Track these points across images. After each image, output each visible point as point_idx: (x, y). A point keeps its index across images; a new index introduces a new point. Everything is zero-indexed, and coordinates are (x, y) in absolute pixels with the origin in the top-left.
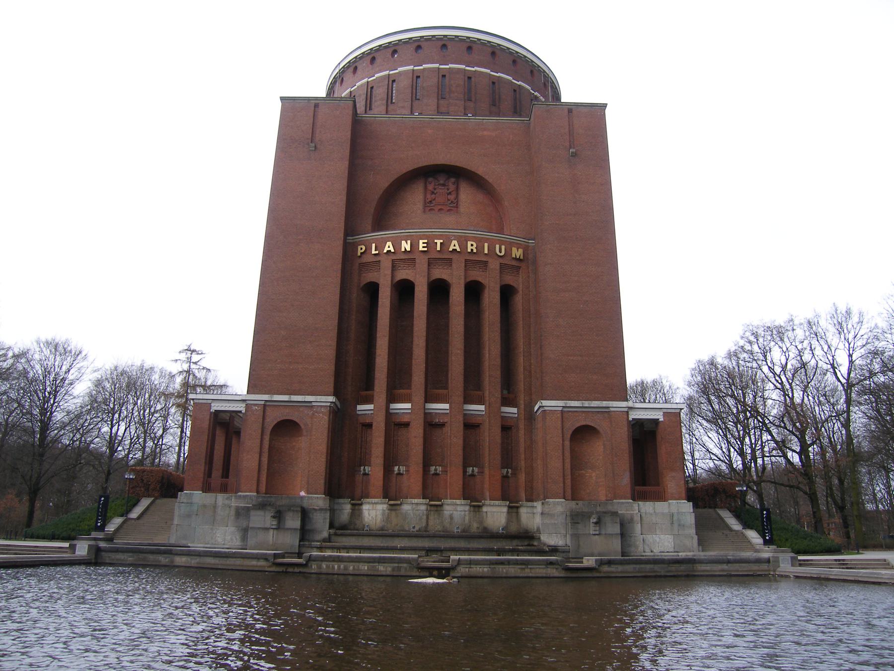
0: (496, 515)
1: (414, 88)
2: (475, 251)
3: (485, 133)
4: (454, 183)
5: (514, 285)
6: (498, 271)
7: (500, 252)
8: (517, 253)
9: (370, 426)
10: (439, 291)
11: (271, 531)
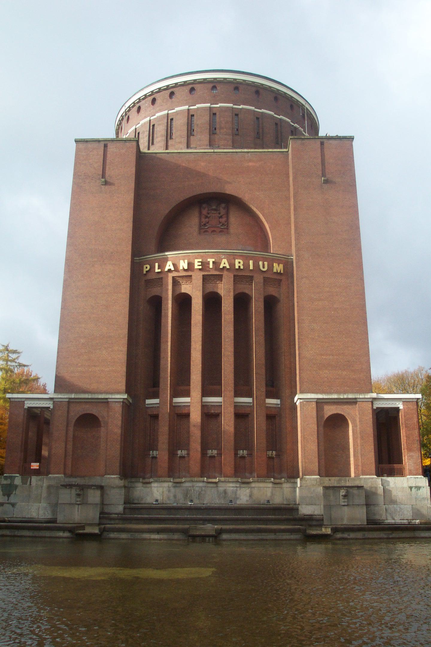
2: (242, 267)
3: (250, 164)
4: (224, 208)
5: (276, 295)
6: (262, 284)
7: (264, 267)
8: (278, 268)
9: (155, 417)
11: (77, 506)
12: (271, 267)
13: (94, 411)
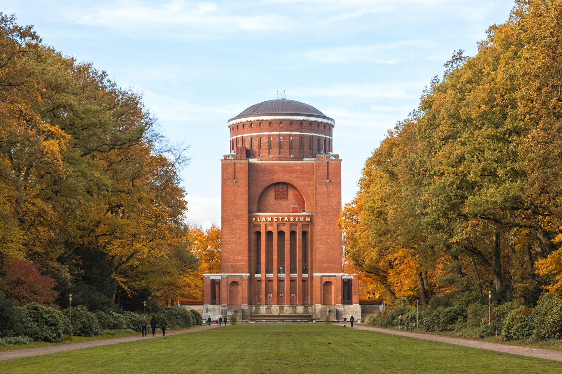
0: (300, 309)
1: (269, 142)
3: (297, 168)
8: (308, 219)
9: (260, 281)
10: (281, 234)
12: (305, 219)
13: (237, 280)
